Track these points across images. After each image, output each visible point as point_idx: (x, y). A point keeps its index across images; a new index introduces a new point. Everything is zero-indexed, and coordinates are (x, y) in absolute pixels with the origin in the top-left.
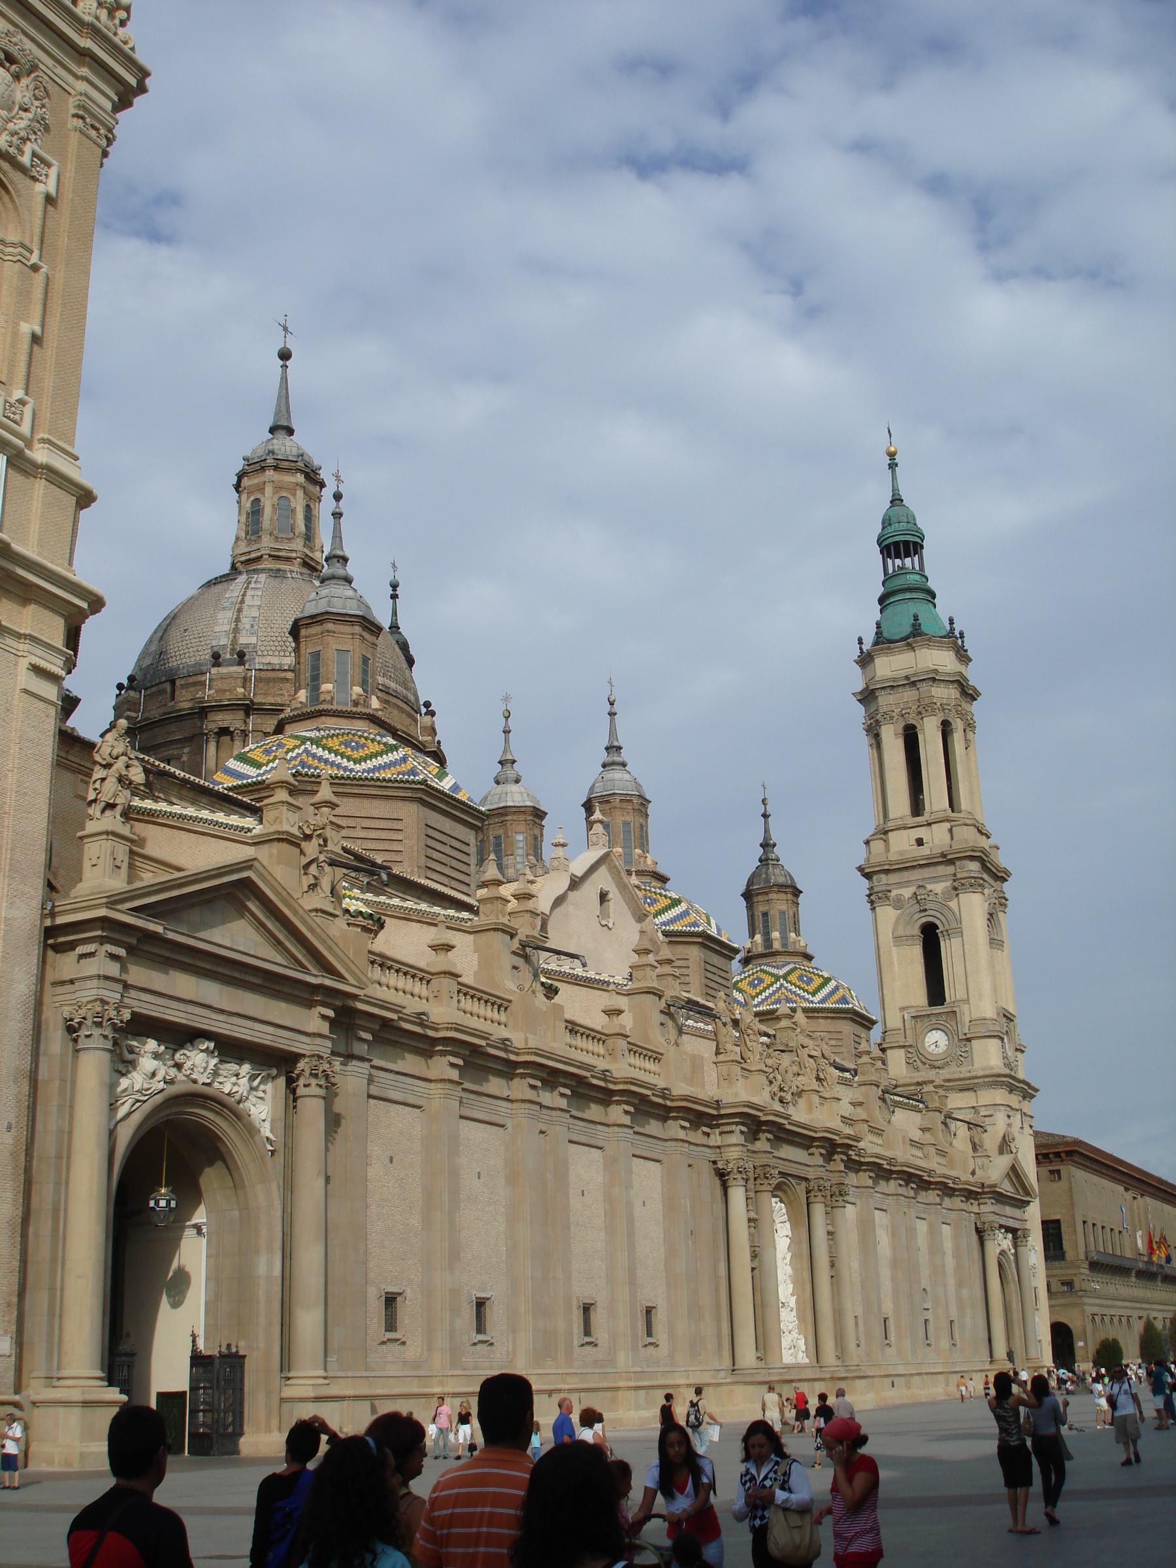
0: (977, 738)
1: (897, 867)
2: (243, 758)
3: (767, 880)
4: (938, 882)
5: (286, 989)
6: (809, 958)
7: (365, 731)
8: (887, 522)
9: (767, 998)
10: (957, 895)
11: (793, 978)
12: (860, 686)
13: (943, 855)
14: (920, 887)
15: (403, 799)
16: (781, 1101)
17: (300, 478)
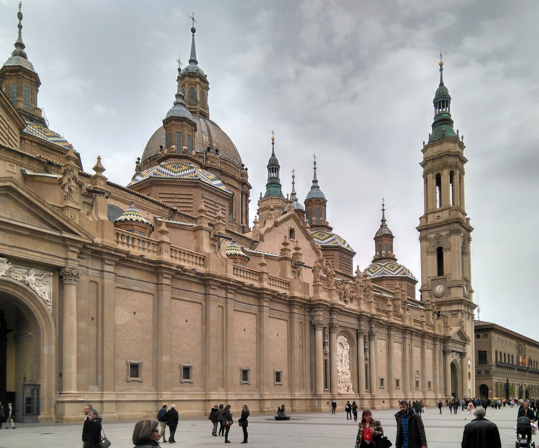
1: (430, 227)
4: (444, 232)
5: (46, 238)
6: (396, 260)
7: (185, 163)
9: (378, 273)
10: (450, 236)
11: (388, 266)
13: (446, 221)
14: (437, 234)
15: (193, 187)
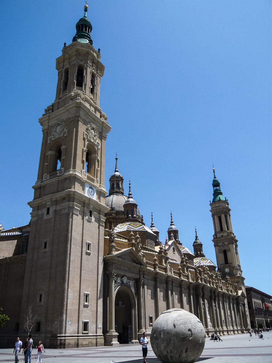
0: (231, 218)
2: (118, 228)
3: (197, 243)
8: (214, 181)
11: (202, 260)
12: (210, 209)
16: (206, 283)
17: (120, 179)
